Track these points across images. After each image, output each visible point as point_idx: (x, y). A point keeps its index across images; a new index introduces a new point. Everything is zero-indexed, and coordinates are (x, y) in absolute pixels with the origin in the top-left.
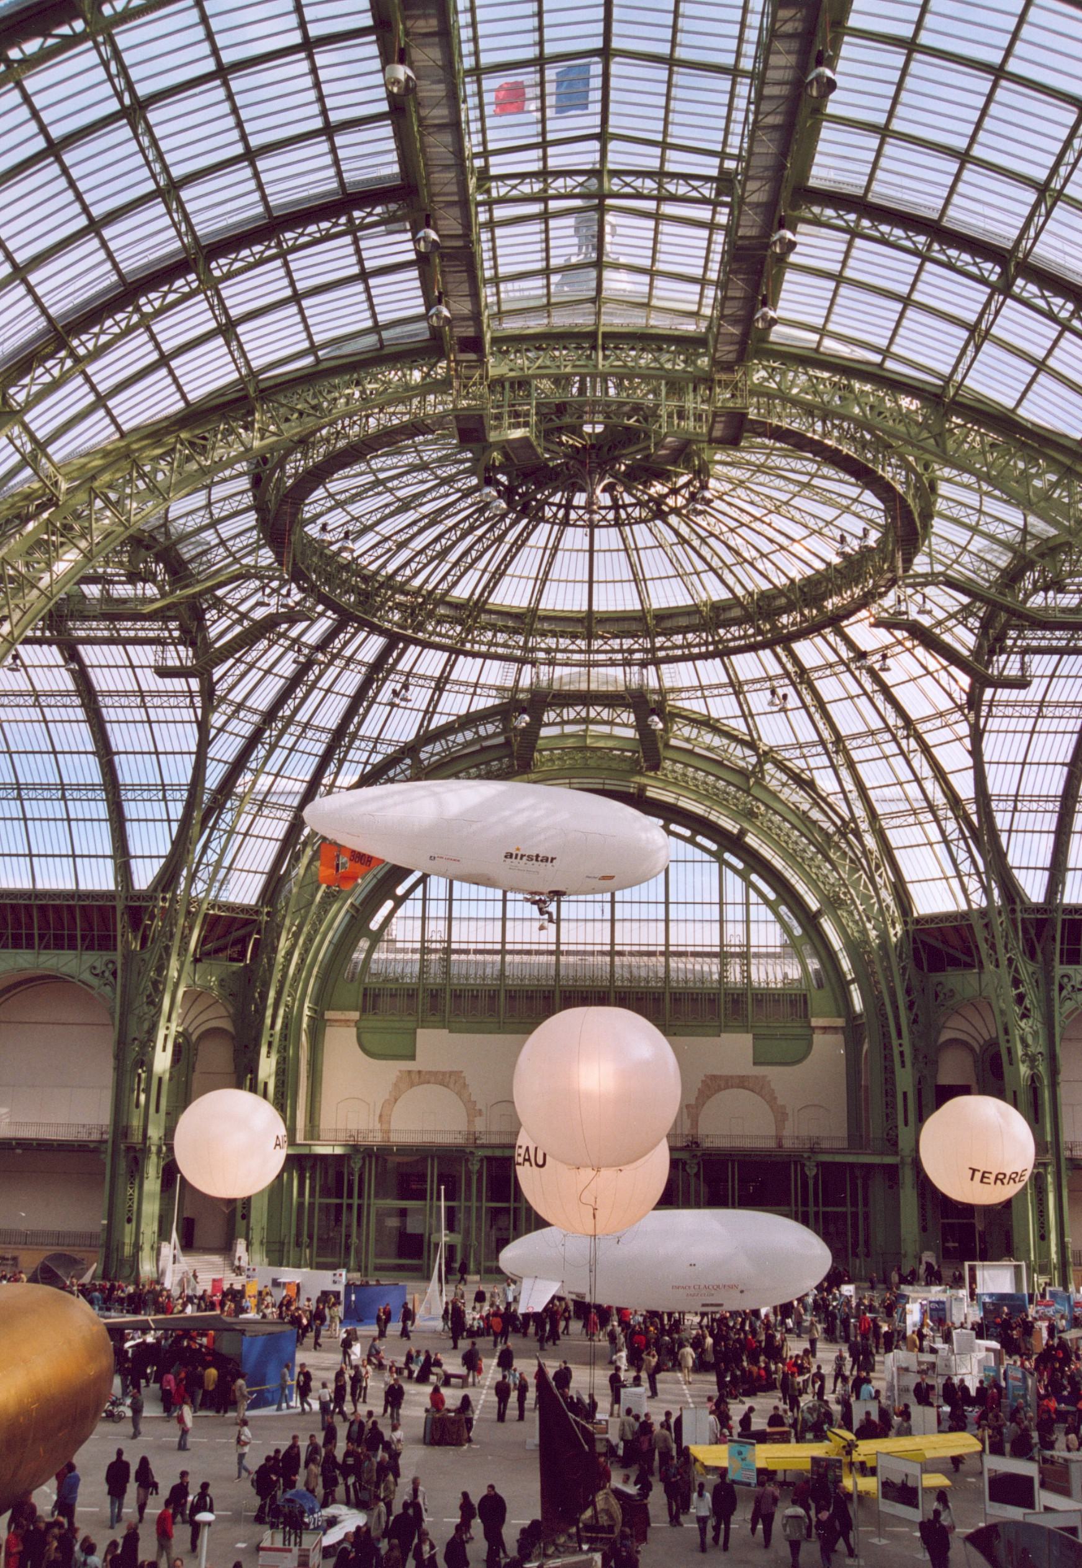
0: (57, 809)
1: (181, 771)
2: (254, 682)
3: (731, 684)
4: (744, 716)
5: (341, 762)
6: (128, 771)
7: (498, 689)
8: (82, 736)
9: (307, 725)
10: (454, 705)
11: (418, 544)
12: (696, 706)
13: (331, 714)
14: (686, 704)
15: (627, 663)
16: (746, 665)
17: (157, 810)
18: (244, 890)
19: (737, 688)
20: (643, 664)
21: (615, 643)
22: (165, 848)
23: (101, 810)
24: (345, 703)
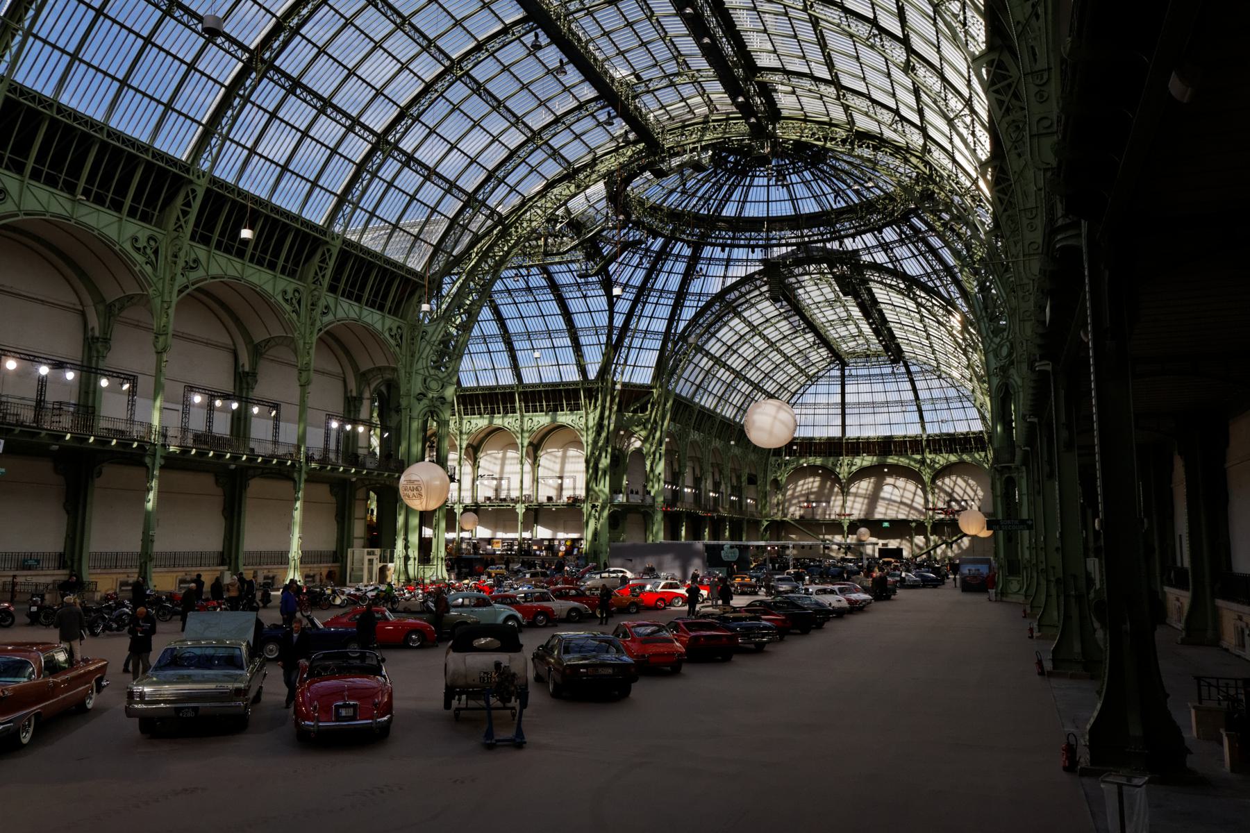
0: (548, 343)
1: (602, 320)
2: (629, 272)
3: (881, 245)
4: (891, 261)
5: (682, 306)
6: (581, 321)
7: (759, 261)
8: (553, 307)
9: (662, 291)
10: (738, 272)
11: (699, 194)
12: (866, 258)
13: (674, 283)
14: (864, 258)
15: (824, 241)
16: (889, 234)
17: (594, 340)
18: (644, 377)
19: (885, 247)
20: (829, 240)
21: (815, 230)
22: (600, 359)
23: (567, 341)
24: (679, 278)
